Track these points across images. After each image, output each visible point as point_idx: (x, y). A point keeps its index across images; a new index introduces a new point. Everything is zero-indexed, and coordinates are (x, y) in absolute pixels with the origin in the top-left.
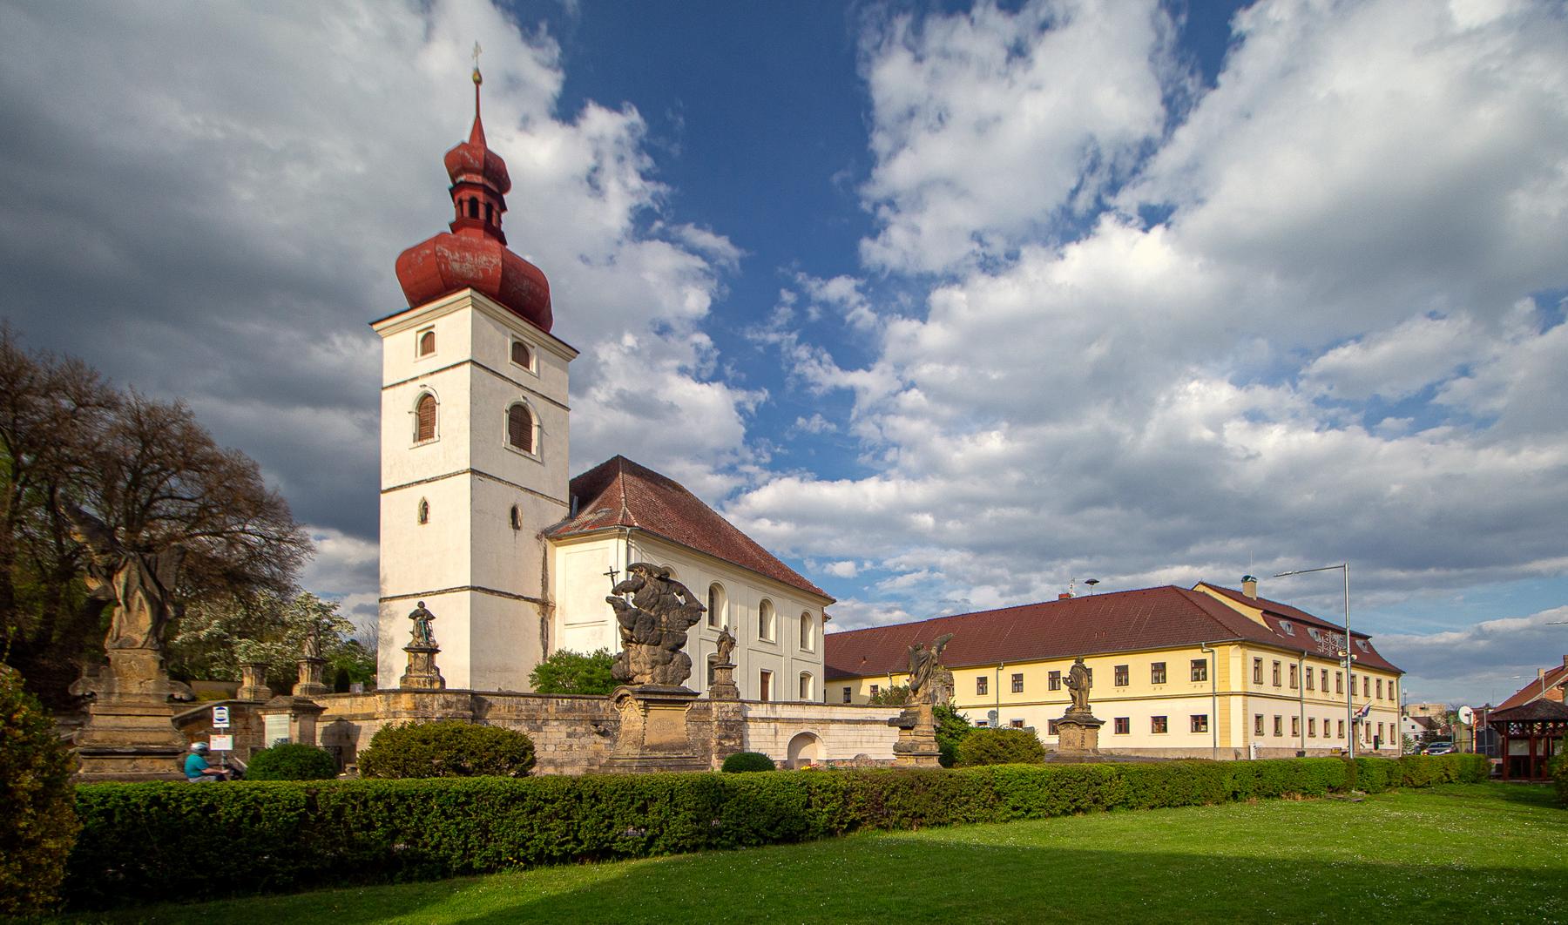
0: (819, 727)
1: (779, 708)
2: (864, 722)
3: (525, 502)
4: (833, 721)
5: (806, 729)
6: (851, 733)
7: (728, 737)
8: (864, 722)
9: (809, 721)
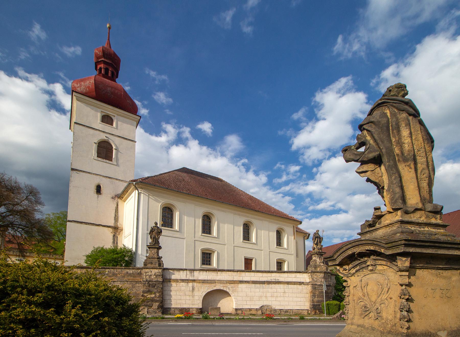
0: (230, 286)
1: (196, 273)
2: (269, 283)
3: (104, 184)
4: (241, 282)
5: (219, 287)
6: (257, 290)
7: (150, 292)
8: (269, 283)
9: (220, 282)
